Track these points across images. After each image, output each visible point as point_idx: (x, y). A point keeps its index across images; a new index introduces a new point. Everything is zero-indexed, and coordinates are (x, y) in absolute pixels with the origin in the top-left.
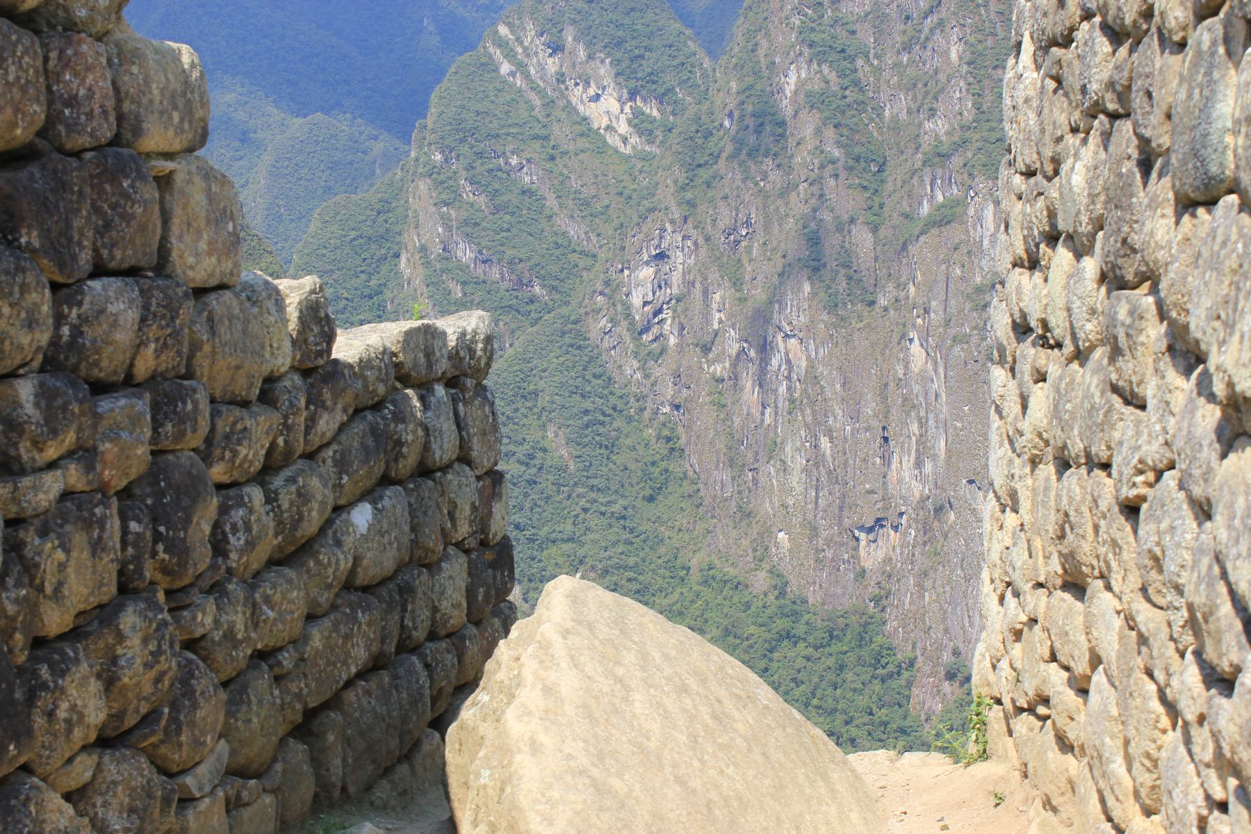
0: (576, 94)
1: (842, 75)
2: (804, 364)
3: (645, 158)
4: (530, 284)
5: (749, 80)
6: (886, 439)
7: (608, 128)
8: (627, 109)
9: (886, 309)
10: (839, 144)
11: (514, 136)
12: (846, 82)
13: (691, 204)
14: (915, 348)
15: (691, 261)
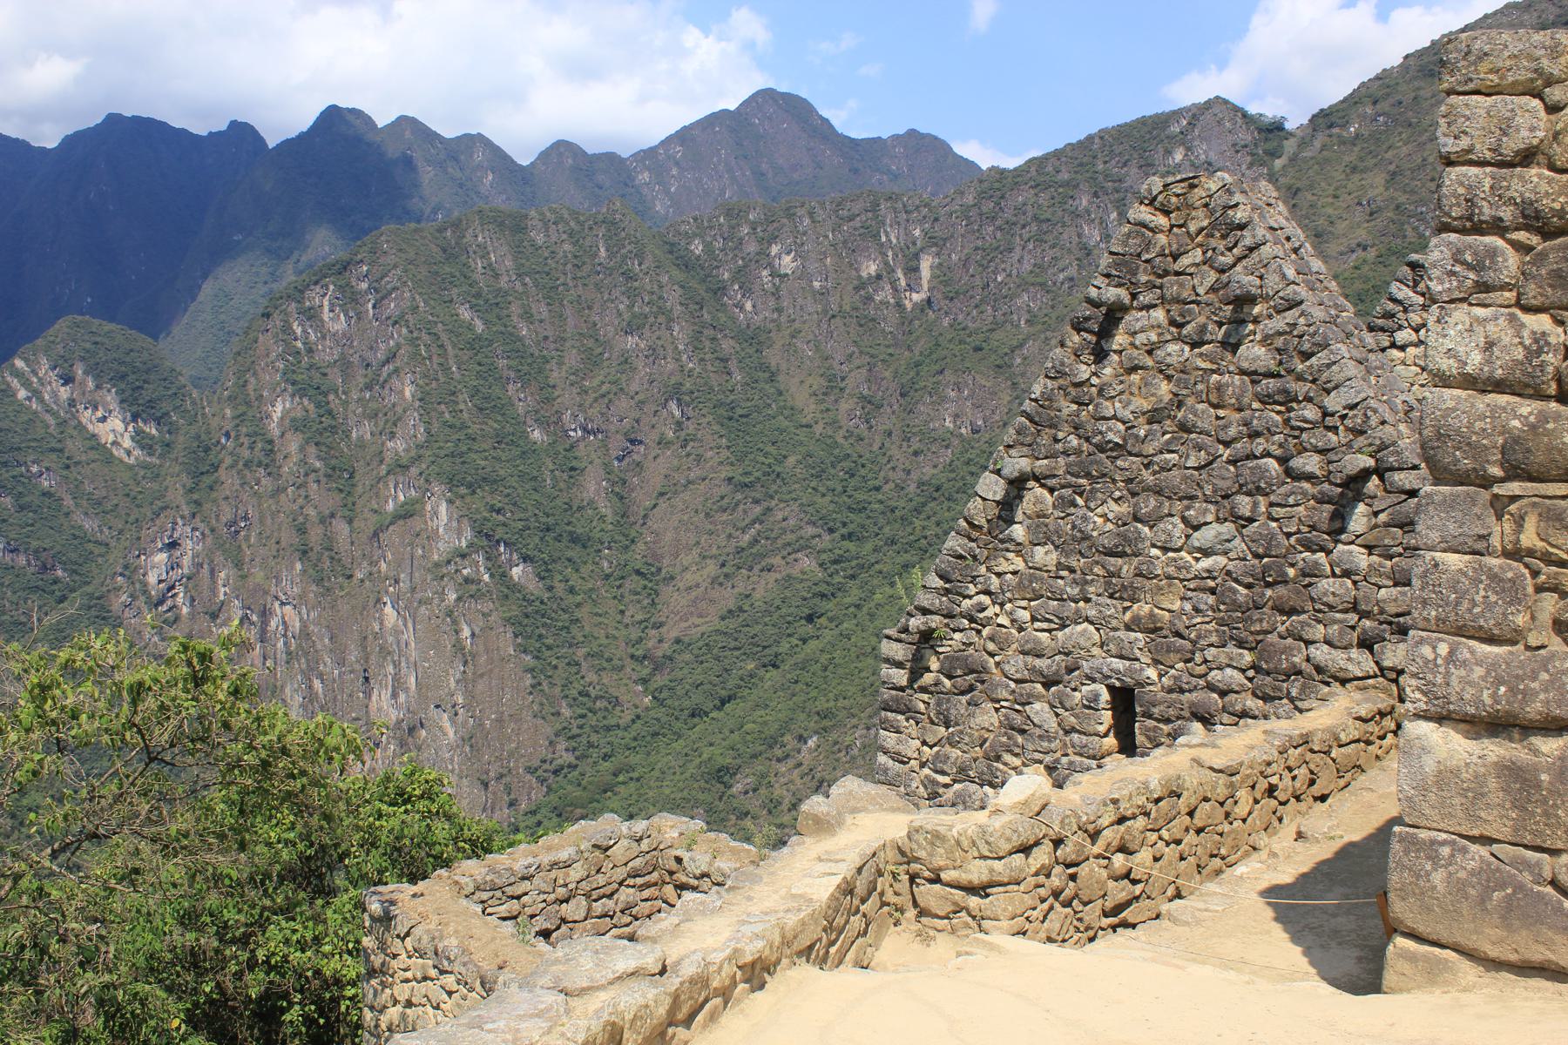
0: (86, 416)
1: (318, 406)
2: (298, 624)
3: (145, 466)
4: (53, 568)
5: (242, 409)
6: (367, 679)
7: (115, 443)
8: (130, 428)
9: (362, 581)
10: (319, 458)
11: (34, 449)
12: (322, 411)
13: (198, 503)
14: (388, 609)
15: (200, 547)
